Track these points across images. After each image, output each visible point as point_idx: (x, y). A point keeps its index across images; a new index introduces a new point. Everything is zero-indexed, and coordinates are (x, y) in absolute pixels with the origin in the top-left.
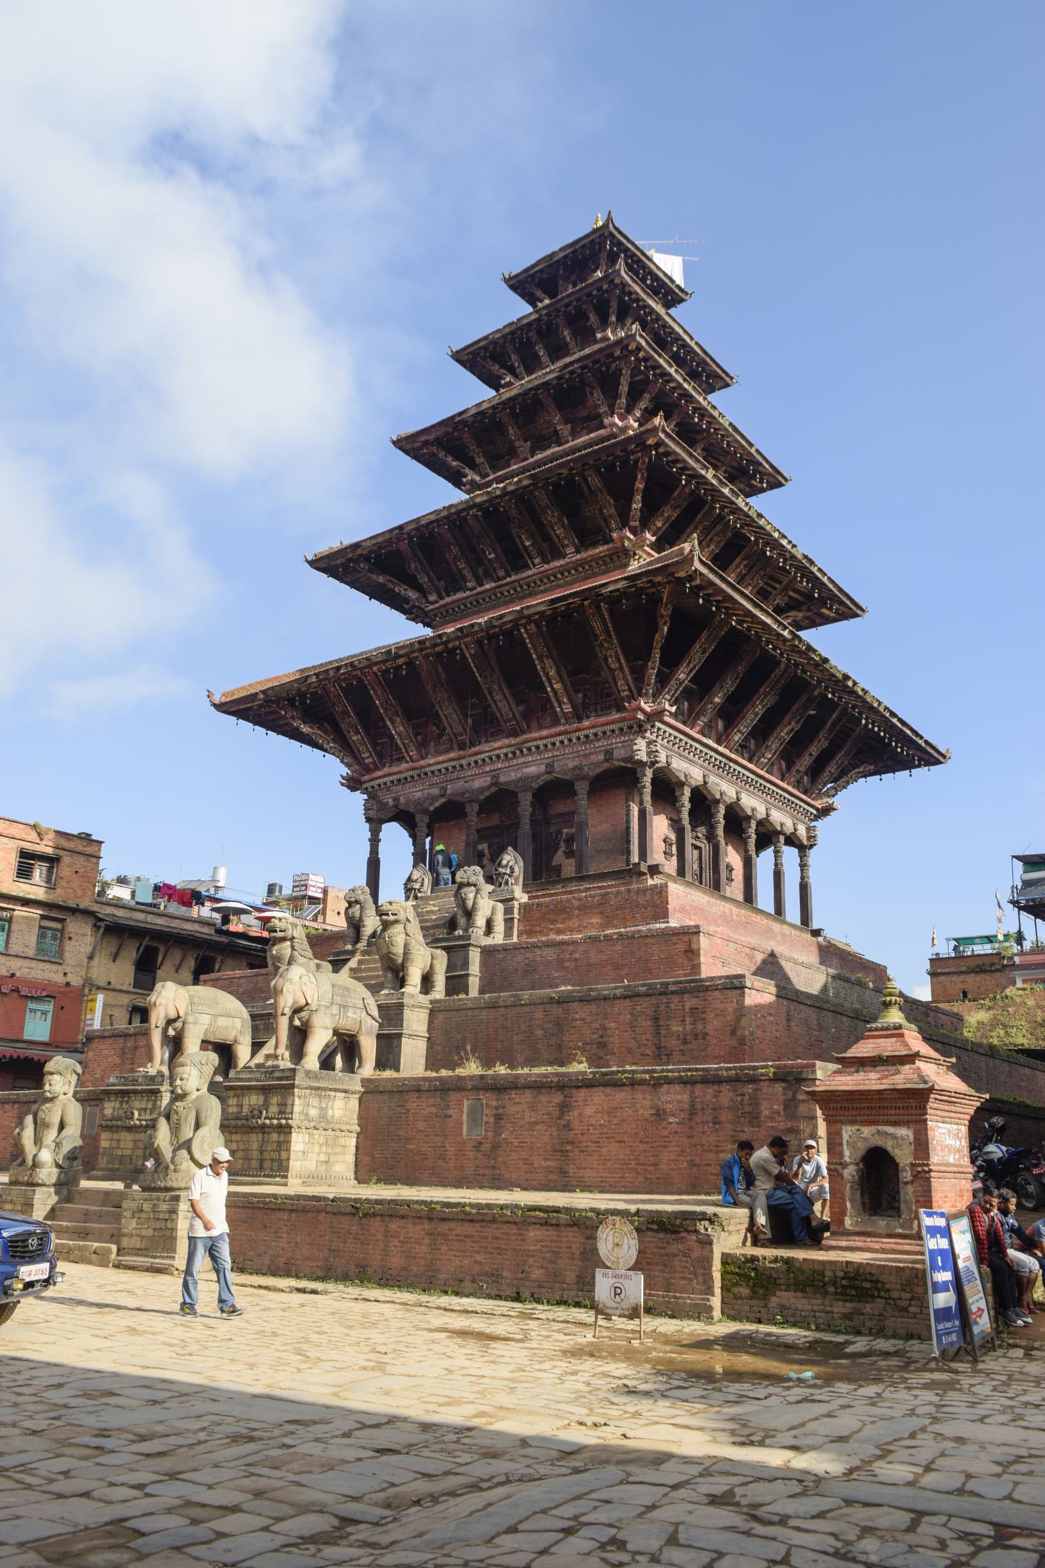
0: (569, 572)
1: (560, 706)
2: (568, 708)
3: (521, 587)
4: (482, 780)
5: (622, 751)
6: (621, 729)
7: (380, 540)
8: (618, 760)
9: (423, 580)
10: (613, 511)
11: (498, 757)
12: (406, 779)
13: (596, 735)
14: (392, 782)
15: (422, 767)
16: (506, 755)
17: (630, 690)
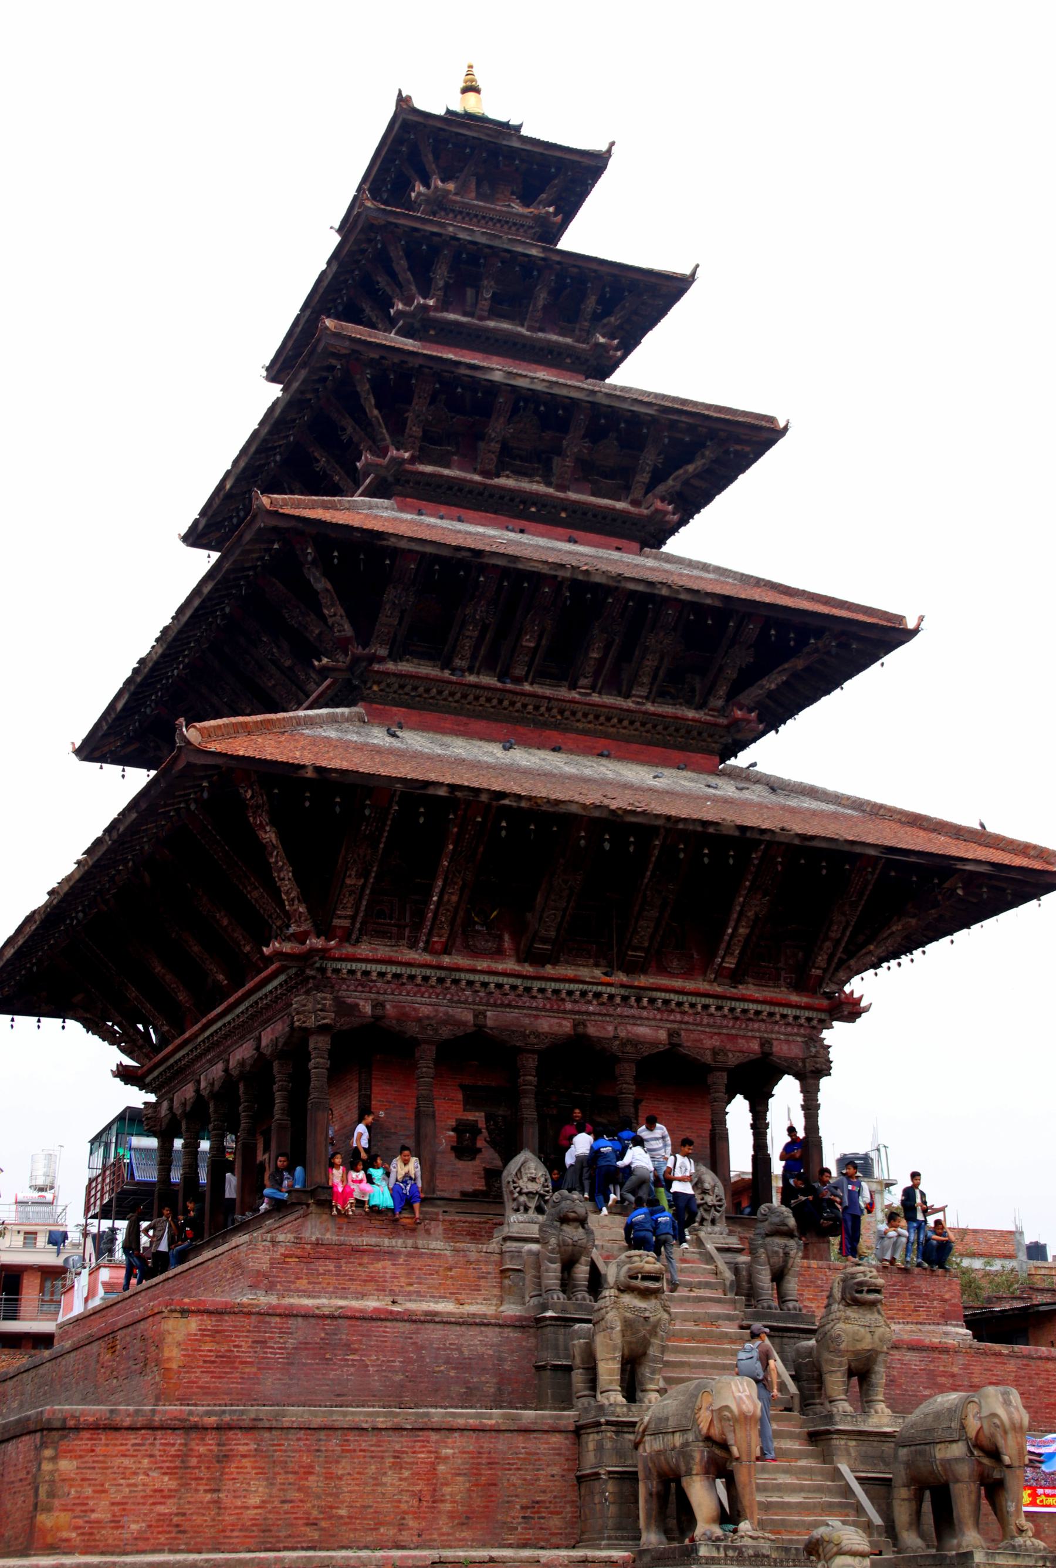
0: (632, 723)
1: (723, 958)
2: (730, 963)
3: (549, 709)
4: (556, 1021)
5: (785, 1047)
6: (796, 1018)
7: (429, 549)
8: (780, 1058)
9: (387, 619)
10: (735, 676)
11: (598, 995)
12: (412, 977)
13: (758, 1013)
14: (381, 975)
15: (459, 969)
16: (611, 997)
17: (825, 970)
